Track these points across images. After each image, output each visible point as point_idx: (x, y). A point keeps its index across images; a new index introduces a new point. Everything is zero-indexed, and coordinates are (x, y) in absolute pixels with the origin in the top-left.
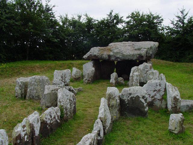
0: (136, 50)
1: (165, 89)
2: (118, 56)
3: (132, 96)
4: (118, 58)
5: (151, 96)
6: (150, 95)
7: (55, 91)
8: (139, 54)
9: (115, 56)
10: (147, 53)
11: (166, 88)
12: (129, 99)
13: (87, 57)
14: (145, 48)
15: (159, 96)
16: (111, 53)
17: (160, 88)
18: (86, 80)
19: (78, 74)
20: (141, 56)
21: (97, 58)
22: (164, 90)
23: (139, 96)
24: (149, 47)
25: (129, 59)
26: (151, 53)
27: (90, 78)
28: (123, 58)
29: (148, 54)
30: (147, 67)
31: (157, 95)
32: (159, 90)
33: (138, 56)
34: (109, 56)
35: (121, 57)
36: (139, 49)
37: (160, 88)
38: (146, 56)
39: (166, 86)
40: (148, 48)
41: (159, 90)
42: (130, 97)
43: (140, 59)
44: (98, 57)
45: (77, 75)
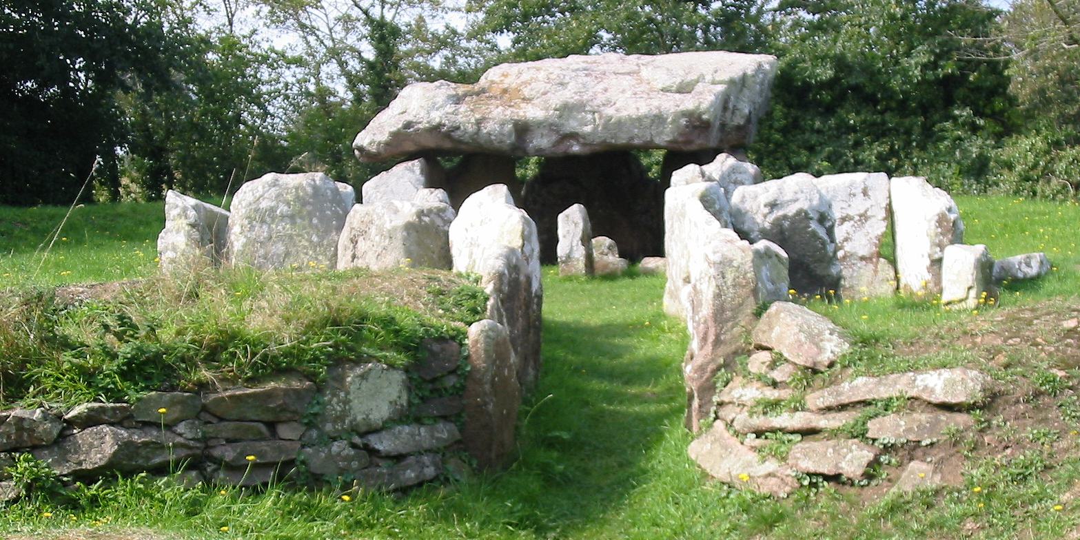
1: (890, 212)
2: (572, 125)
3: (779, 213)
4: (574, 136)
7: (432, 216)
8: (689, 115)
10: (725, 108)
11: (890, 205)
12: (767, 225)
13: (384, 137)
14: (714, 83)
15: (864, 241)
16: (532, 113)
17: (868, 204)
20: (696, 123)
21: (447, 145)
22: (883, 214)
23: (806, 213)
25: (636, 142)
26: (747, 111)
28: (602, 136)
29: (728, 115)
31: (856, 237)
32: (864, 217)
33: (683, 121)
34: (523, 129)
35: (588, 129)
36: (684, 89)
37: (868, 204)
38: (723, 126)
39: (890, 197)
40: (732, 82)
41: (860, 216)
42: (771, 218)
44: (459, 133)
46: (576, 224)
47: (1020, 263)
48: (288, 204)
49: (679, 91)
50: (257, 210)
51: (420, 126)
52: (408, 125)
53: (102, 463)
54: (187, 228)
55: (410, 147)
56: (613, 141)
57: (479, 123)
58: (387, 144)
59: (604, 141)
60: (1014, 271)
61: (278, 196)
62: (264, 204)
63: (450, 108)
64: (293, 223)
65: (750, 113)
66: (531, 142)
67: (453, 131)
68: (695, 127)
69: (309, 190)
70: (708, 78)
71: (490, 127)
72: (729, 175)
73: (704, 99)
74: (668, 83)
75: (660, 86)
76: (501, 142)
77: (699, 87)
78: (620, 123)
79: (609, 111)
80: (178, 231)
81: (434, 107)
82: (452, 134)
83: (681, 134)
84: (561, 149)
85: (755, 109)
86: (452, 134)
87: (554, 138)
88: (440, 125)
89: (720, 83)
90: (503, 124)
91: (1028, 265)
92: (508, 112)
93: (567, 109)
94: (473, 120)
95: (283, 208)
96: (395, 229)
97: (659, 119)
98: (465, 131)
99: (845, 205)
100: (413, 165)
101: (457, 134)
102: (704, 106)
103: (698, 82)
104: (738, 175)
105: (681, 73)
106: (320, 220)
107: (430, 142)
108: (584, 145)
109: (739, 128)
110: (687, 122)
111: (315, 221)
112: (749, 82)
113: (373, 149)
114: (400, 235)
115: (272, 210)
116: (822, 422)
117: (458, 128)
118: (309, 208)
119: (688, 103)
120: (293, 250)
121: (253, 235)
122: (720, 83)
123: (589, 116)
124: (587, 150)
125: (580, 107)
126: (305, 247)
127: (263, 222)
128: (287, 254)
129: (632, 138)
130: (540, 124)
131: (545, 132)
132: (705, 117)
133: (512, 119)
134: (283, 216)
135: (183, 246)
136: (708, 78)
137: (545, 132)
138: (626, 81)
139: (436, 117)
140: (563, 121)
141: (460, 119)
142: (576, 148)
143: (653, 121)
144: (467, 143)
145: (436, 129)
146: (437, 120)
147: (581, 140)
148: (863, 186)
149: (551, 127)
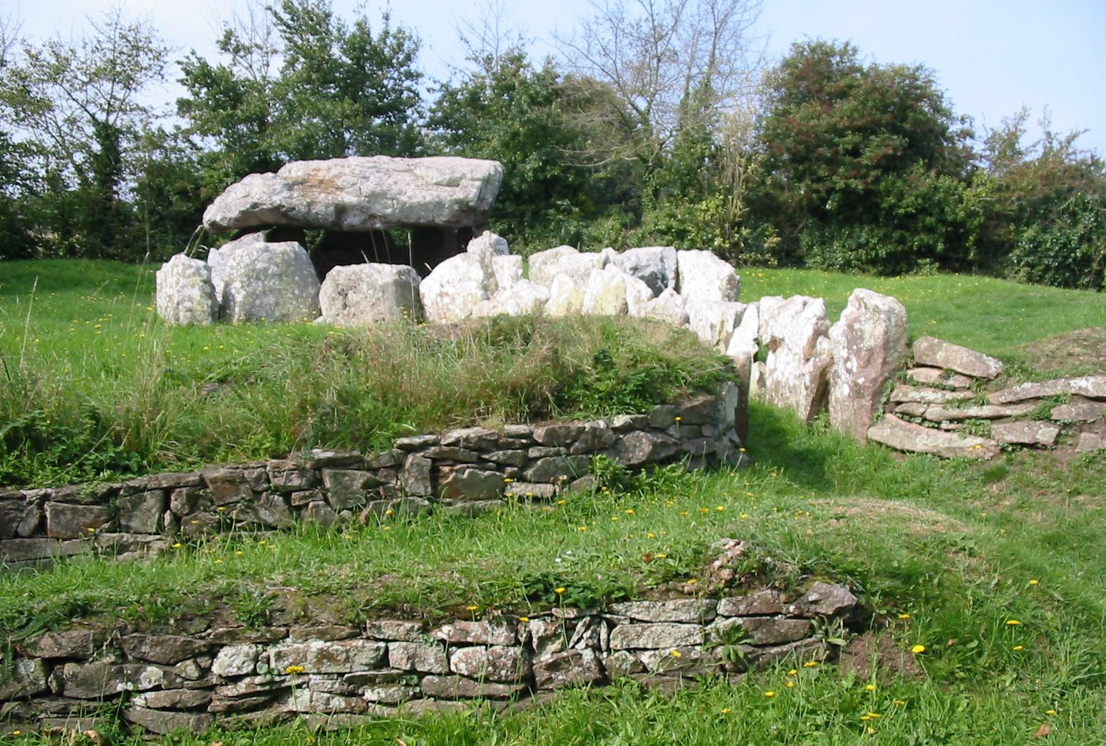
0: (438, 184)
2: (377, 209)
8: (461, 203)
11: (677, 269)
14: (473, 180)
16: (348, 198)
20: (465, 208)
21: (283, 221)
25: (422, 221)
28: (398, 216)
33: (456, 207)
34: (341, 210)
35: (389, 211)
36: (453, 183)
39: (677, 263)
44: (294, 212)
48: (277, 265)
49: (449, 185)
50: (254, 270)
52: (255, 205)
53: (644, 459)
54: (201, 284)
55: (254, 222)
57: (309, 205)
58: (236, 220)
61: (270, 259)
62: (259, 266)
63: (286, 194)
64: (281, 280)
68: (463, 211)
69: (292, 255)
70: (469, 176)
71: (318, 208)
73: (469, 191)
74: (440, 179)
75: (434, 181)
76: (325, 219)
77: (463, 182)
78: (412, 207)
79: (404, 198)
80: (193, 286)
81: (274, 192)
83: (453, 216)
84: (369, 225)
87: (363, 217)
88: (281, 206)
89: (477, 180)
90: (327, 206)
92: (330, 198)
93: (374, 196)
95: (273, 269)
96: (386, 285)
97: (439, 205)
98: (299, 211)
102: (471, 196)
103: (461, 178)
106: (300, 277)
107: (270, 219)
108: (384, 223)
111: (297, 278)
113: (225, 224)
114: (391, 289)
115: (266, 270)
116: (1008, 411)
118: (292, 269)
119: (459, 194)
120: (281, 301)
121: (250, 289)
122: (477, 180)
123: (390, 202)
125: (383, 195)
126: (290, 299)
127: (258, 278)
128: (277, 304)
130: (354, 207)
131: (357, 213)
132: (471, 204)
134: (273, 275)
135: (198, 298)
136: (469, 176)
137: (357, 213)
138: (407, 177)
139: (277, 200)
141: (295, 202)
144: (299, 220)
145: (277, 209)
146: (278, 202)
149: (361, 209)
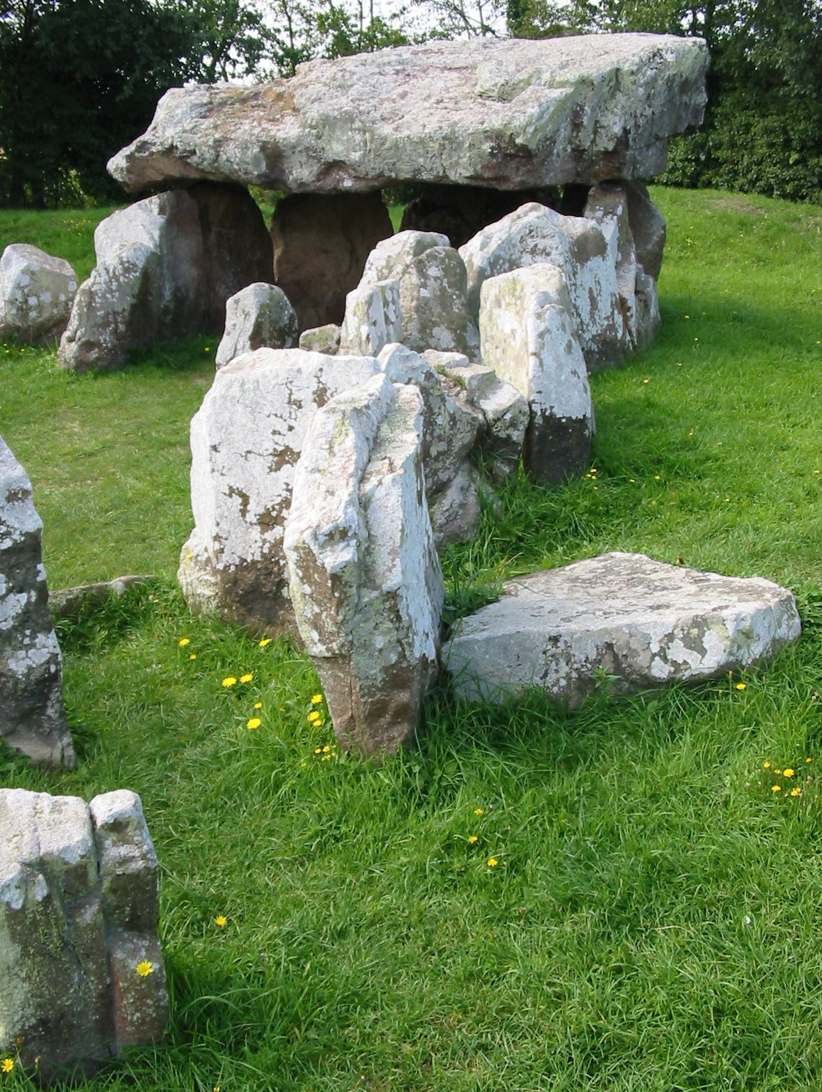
2: (335, 150)
5: (255, 509)
6: (245, 499)
9: (312, 153)
10: (577, 126)
14: (551, 85)
16: (288, 130)
18: (71, 340)
19: (47, 298)
20: (509, 151)
24: (604, 65)
25: (425, 176)
26: (617, 130)
27: (105, 325)
28: (374, 167)
30: (542, 244)
33: (487, 147)
35: (356, 156)
43: (507, 172)
45: (33, 301)
46: (246, 315)
47: (670, 637)
51: (154, 149)
55: (153, 176)
56: (393, 175)
57: (218, 144)
59: (381, 175)
60: (641, 660)
65: (626, 131)
66: (291, 173)
67: (188, 157)
70: (546, 76)
71: (231, 152)
72: (522, 240)
79: (386, 129)
82: (189, 160)
85: (637, 126)
86: (189, 160)
88: (172, 148)
89: (562, 84)
91: (696, 645)
94: (211, 143)
97: (451, 141)
99: (283, 427)
100: (151, 201)
101: (194, 160)
102: (520, 121)
104: (538, 240)
105: (512, 68)
107: (174, 171)
108: (357, 178)
109: (606, 154)
110: (492, 148)
112: (627, 81)
117: (194, 152)
119: (497, 117)
122: (562, 84)
123: (358, 137)
124: (361, 186)
129: (418, 171)
132: (519, 141)
133: (259, 141)
140: (321, 144)
142: (348, 183)
143: (443, 147)
147: (352, 172)
148: (314, 387)
